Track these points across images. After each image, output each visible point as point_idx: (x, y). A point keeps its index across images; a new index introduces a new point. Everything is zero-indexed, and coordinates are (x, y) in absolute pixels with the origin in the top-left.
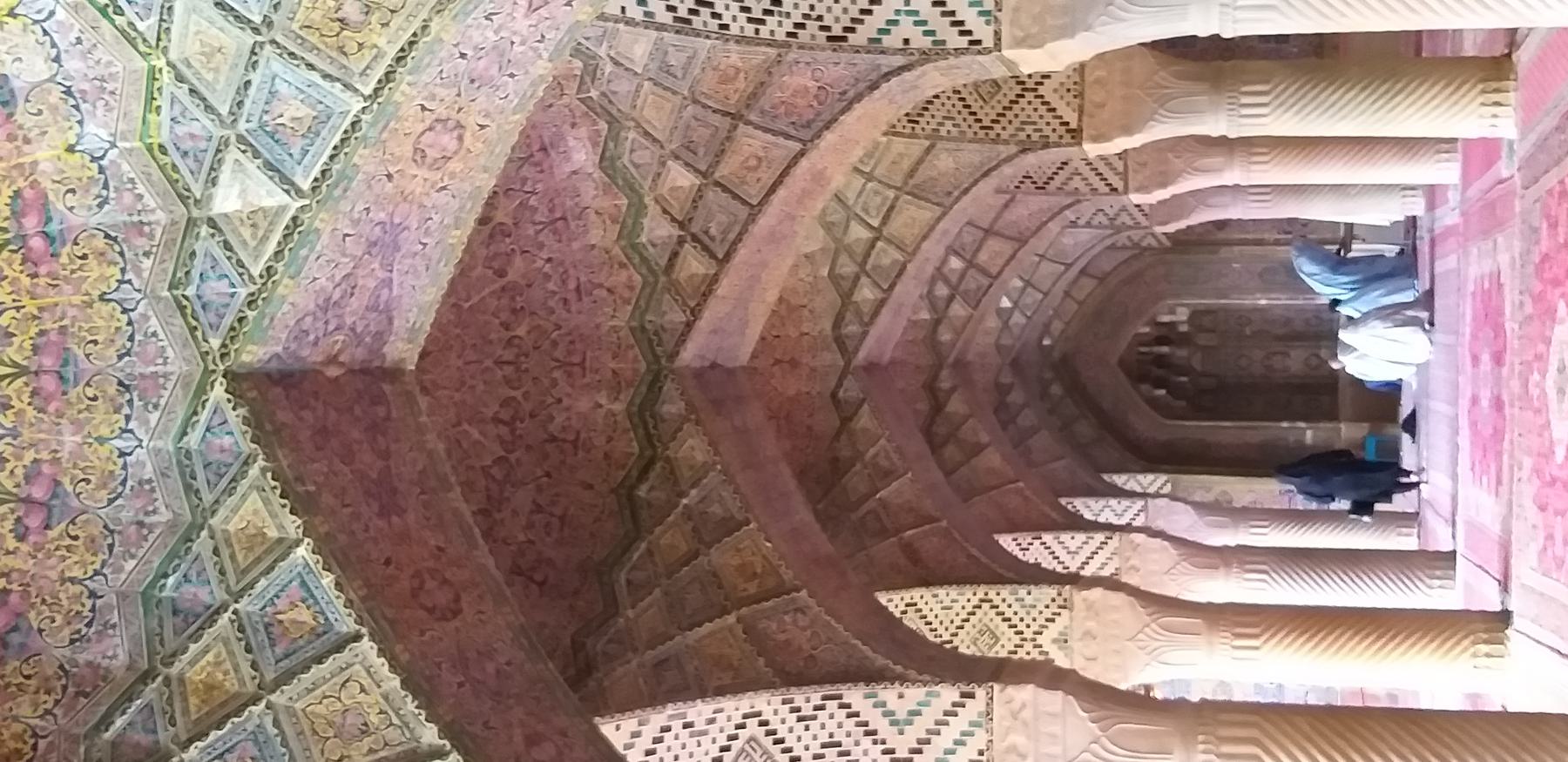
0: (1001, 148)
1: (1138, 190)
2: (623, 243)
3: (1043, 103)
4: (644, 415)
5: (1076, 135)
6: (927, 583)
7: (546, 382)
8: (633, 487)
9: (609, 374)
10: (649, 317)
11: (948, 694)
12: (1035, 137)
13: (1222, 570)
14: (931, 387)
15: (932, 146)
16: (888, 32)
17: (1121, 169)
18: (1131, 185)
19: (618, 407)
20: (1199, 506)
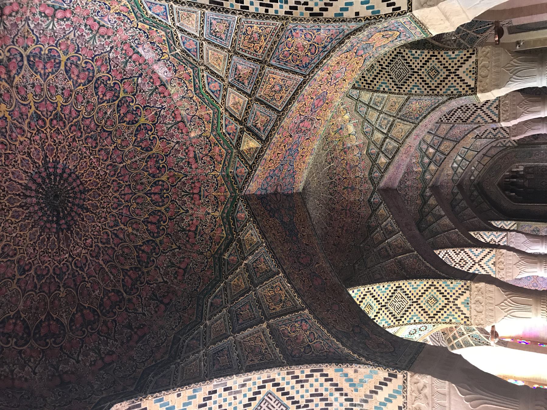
0: (440, 98)
1: (504, 121)
2: (214, 133)
3: (458, 78)
4: (230, 219)
5: (474, 91)
6: (406, 279)
7: (179, 203)
8: (222, 254)
9: (213, 198)
10: (230, 170)
11: (382, 374)
12: (455, 92)
13: (539, 264)
14: (422, 195)
15: (409, 98)
16: (347, 9)
17: (497, 113)
18: (501, 119)
19: (217, 214)
20: (527, 234)
